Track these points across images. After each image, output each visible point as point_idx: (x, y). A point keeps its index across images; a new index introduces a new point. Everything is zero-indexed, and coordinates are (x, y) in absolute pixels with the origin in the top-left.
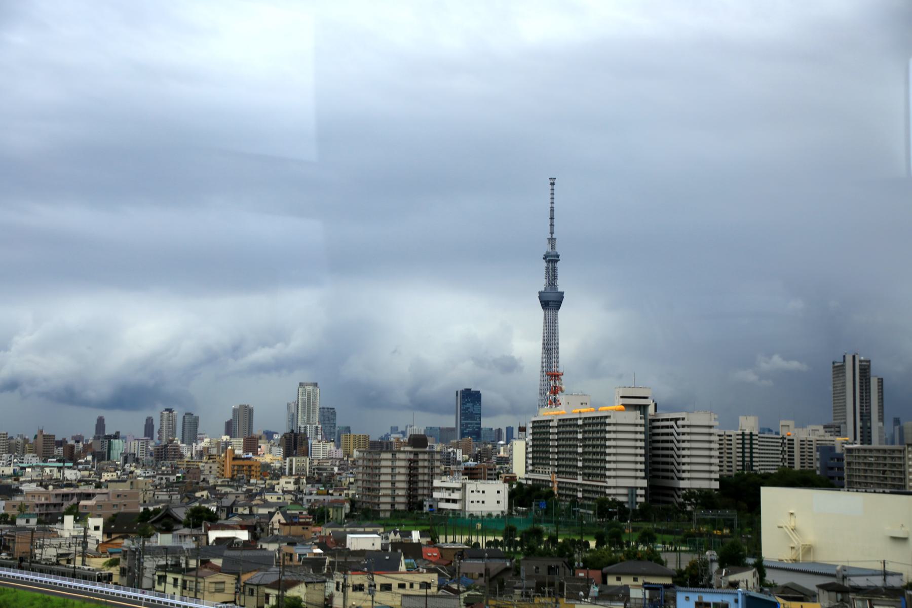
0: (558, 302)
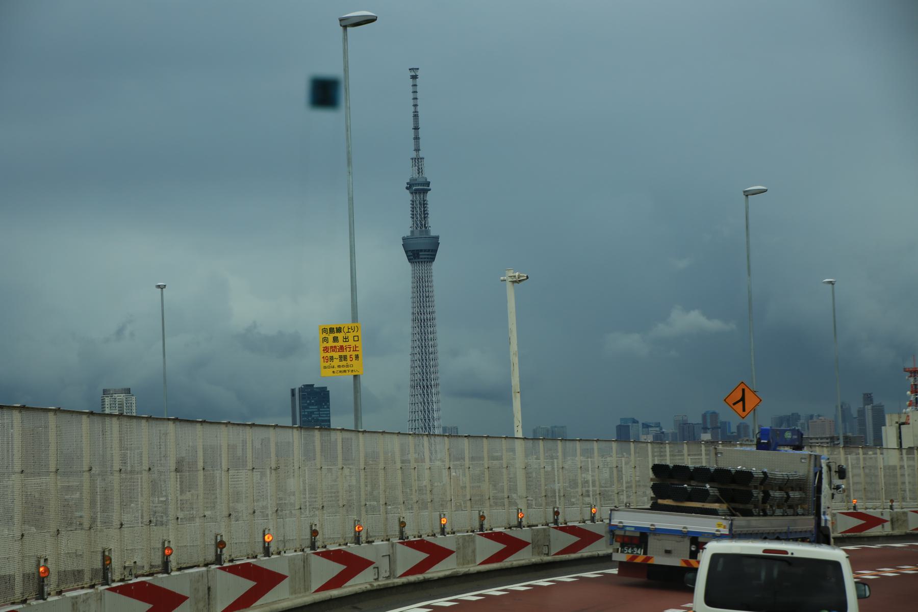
0: (432, 251)
